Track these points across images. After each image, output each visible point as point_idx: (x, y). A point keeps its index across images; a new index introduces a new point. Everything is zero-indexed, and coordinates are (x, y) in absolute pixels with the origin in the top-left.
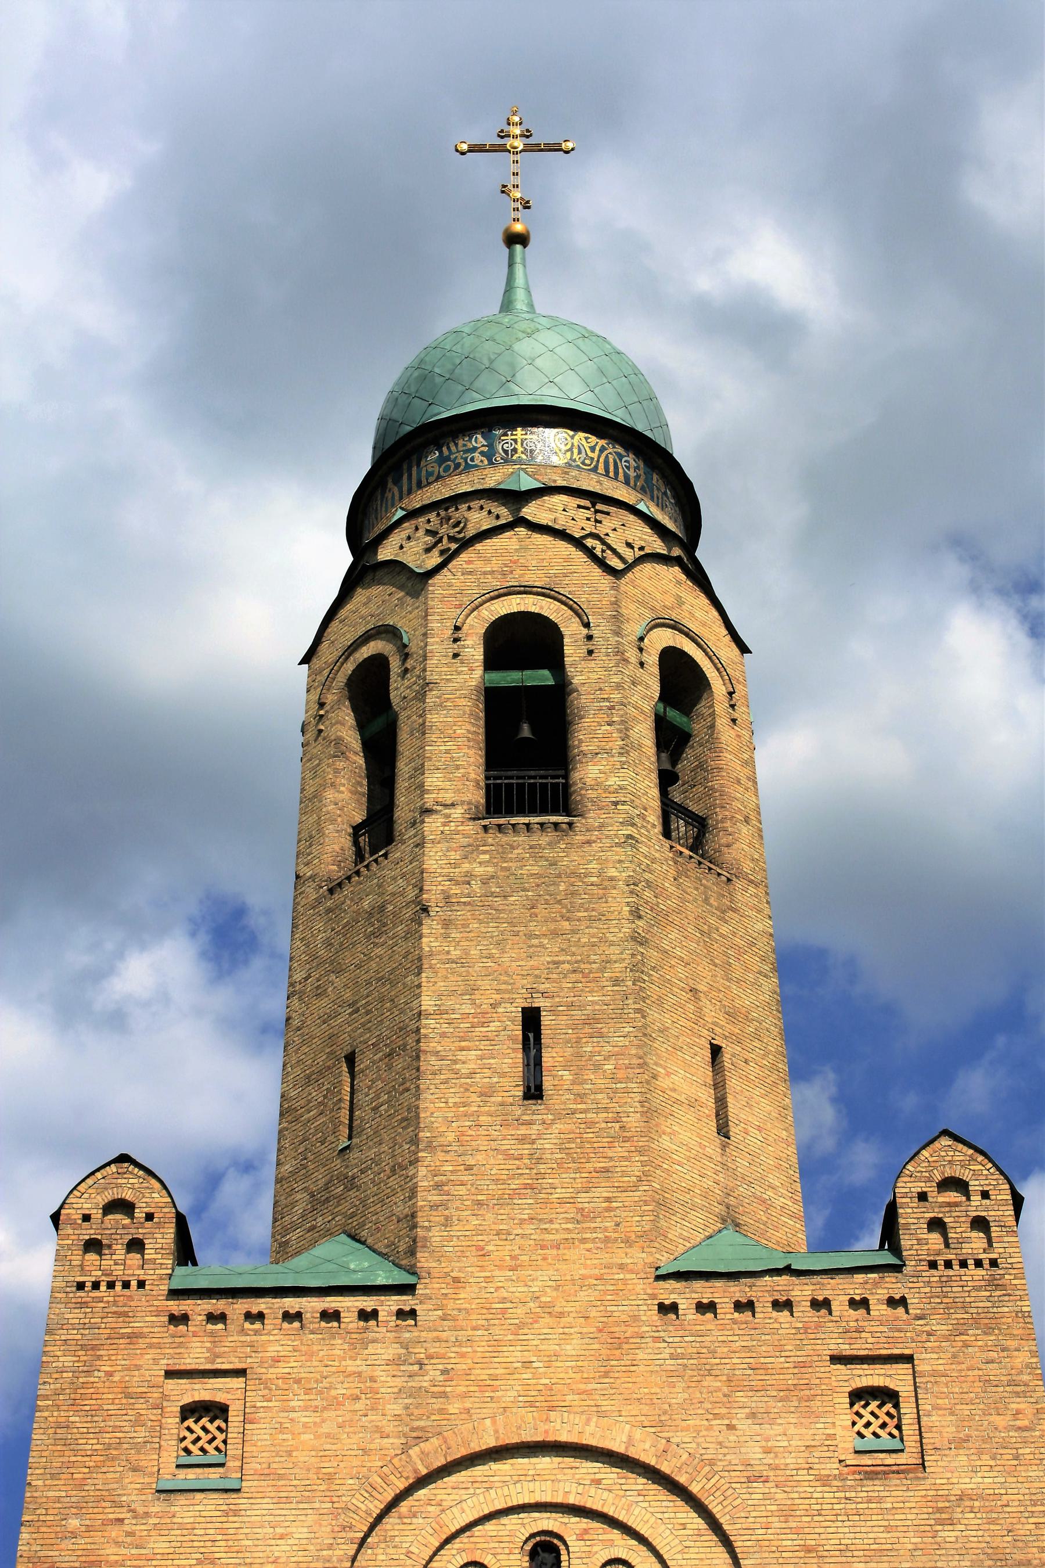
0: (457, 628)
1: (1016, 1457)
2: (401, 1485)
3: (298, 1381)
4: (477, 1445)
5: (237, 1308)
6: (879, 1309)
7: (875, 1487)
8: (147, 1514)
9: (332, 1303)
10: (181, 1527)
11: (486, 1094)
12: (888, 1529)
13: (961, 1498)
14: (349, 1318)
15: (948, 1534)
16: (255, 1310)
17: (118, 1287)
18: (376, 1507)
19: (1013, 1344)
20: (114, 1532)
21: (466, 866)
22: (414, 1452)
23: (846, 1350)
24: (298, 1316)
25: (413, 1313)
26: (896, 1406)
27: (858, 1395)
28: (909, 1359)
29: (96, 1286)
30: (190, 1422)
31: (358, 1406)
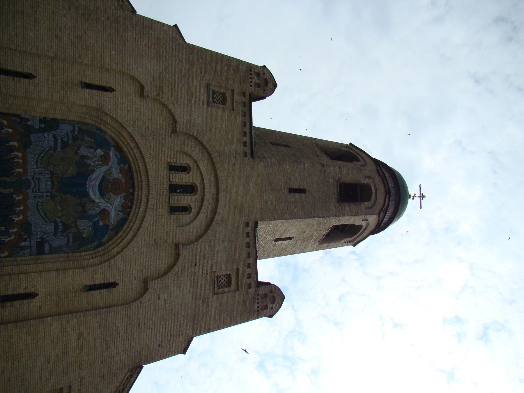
0: (370, 177)
1: (218, 320)
2: (209, 150)
3: (232, 124)
4: (218, 171)
5: (247, 110)
6: (249, 281)
7: (210, 281)
8: (203, 80)
9: (248, 135)
11: (290, 178)
12: (201, 285)
13: (208, 305)
14: (245, 139)
15: (200, 302)
16: (246, 115)
17: (250, 80)
18: (204, 142)
19: (242, 317)
22: (216, 154)
23: (240, 272)
24: (245, 126)
25: (246, 156)
26: (227, 287)
27: (229, 276)
28: (238, 290)
29: (251, 74)
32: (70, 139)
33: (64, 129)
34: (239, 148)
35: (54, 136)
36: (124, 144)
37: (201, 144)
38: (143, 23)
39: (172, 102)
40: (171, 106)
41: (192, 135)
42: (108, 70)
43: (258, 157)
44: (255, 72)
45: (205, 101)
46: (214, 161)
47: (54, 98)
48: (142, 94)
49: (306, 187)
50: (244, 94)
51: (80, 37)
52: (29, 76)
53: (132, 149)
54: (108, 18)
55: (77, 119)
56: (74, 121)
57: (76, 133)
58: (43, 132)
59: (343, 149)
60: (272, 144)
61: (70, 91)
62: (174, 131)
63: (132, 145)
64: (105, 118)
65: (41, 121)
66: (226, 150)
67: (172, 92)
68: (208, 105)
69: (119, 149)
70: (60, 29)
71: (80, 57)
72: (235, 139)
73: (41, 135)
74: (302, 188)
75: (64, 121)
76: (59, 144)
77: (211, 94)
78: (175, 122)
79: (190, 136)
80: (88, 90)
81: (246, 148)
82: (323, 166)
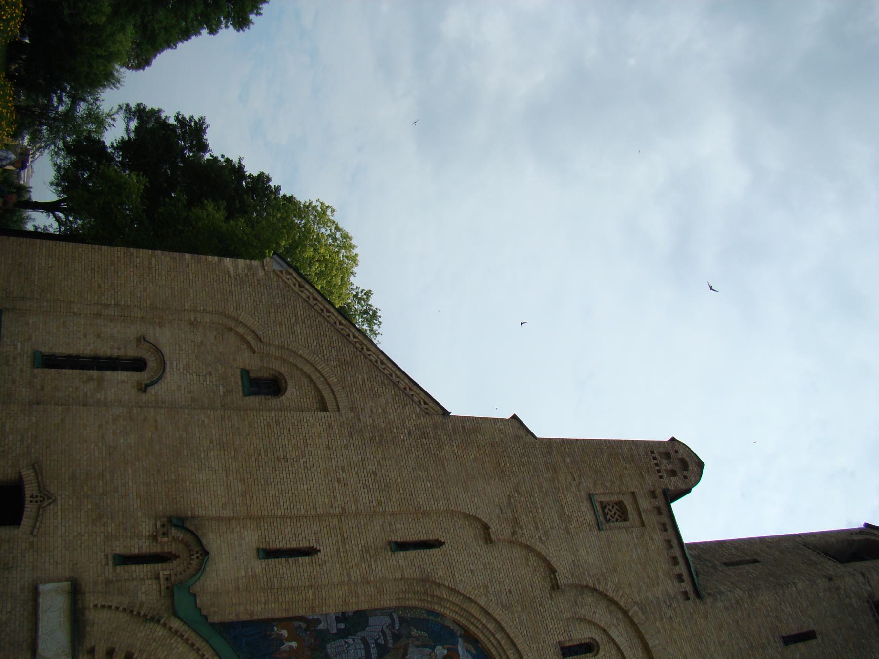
2: (622, 604)
3: (648, 550)
4: (647, 637)
5: (665, 519)
8: (579, 491)
10: (579, 506)
16: (668, 527)
17: (657, 468)
18: (610, 593)
20: (570, 478)
21: (852, 595)
22: (636, 608)
24: (671, 547)
25: (688, 599)
29: (655, 459)
30: (616, 507)
31: (646, 579)
32: (389, 638)
33: (378, 624)
34: (672, 587)
35: (364, 640)
36: (477, 627)
37: (605, 596)
38: (464, 427)
39: (540, 538)
40: (539, 547)
41: (587, 586)
42: (425, 514)
43: (709, 594)
44: (660, 453)
45: (593, 522)
46: (636, 621)
47: (353, 578)
48: (488, 539)
49: (812, 627)
50: (653, 494)
51: (375, 474)
52: (309, 552)
53: (493, 635)
54: (410, 434)
55: (394, 603)
56: (389, 608)
57: (397, 626)
58: (346, 637)
59: (855, 538)
60: (726, 564)
61: (375, 561)
62: (555, 586)
63: (491, 626)
64: (437, 592)
65: (338, 620)
66: (650, 598)
67: (535, 523)
68: (599, 529)
69: (471, 639)
70: (343, 469)
71: (380, 503)
72: (660, 573)
73: (342, 642)
74: (805, 630)
75: (375, 612)
76: (373, 651)
77: (599, 509)
78: (553, 571)
79: (583, 588)
80: (402, 554)
81: (683, 585)
82: (830, 579)
